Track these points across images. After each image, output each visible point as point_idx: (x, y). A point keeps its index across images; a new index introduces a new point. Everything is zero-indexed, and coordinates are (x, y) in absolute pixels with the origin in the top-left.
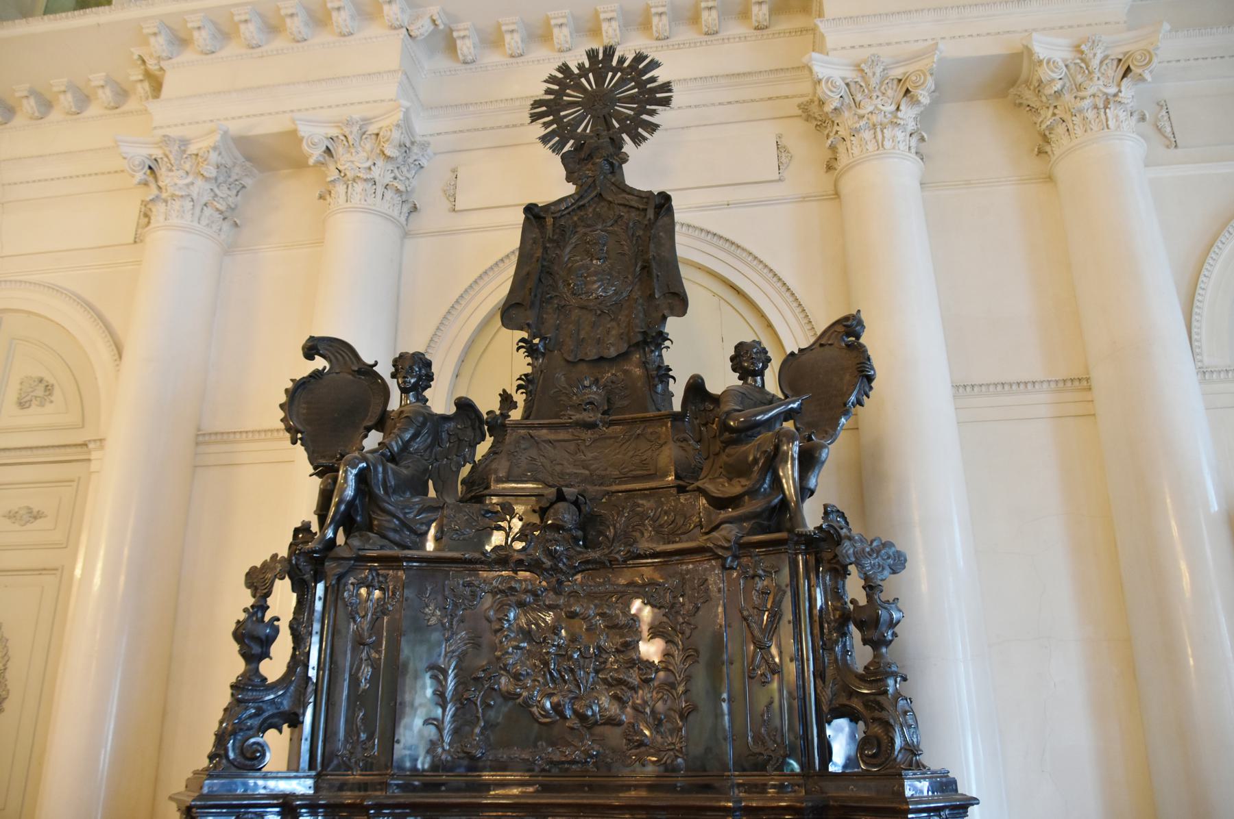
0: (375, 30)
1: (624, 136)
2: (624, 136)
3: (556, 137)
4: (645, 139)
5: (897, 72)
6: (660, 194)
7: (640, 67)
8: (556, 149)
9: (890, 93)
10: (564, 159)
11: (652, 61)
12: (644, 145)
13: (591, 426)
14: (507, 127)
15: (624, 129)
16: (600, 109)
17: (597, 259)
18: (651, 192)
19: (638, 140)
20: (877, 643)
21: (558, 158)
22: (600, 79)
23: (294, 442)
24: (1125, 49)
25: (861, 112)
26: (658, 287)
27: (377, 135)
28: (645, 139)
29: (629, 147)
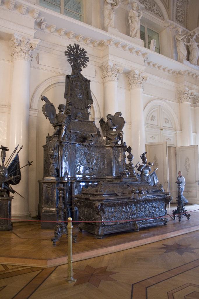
0: (29, 16)
1: (82, 65)
2: (82, 65)
3: (71, 61)
4: (85, 67)
5: (118, 68)
6: (89, 80)
7: (83, 52)
8: (71, 63)
9: (116, 71)
10: (72, 66)
11: (85, 51)
12: (85, 68)
13: (81, 121)
14: (49, 48)
15: (82, 64)
16: (77, 57)
17: (78, 88)
18: (87, 79)
19: (84, 67)
20: (130, 161)
21: (70, 66)
22: (80, 54)
23: (47, 118)
24: (144, 76)
25: (113, 73)
26: (88, 98)
27: (30, 44)
28: (85, 67)
29: (82, 68)
